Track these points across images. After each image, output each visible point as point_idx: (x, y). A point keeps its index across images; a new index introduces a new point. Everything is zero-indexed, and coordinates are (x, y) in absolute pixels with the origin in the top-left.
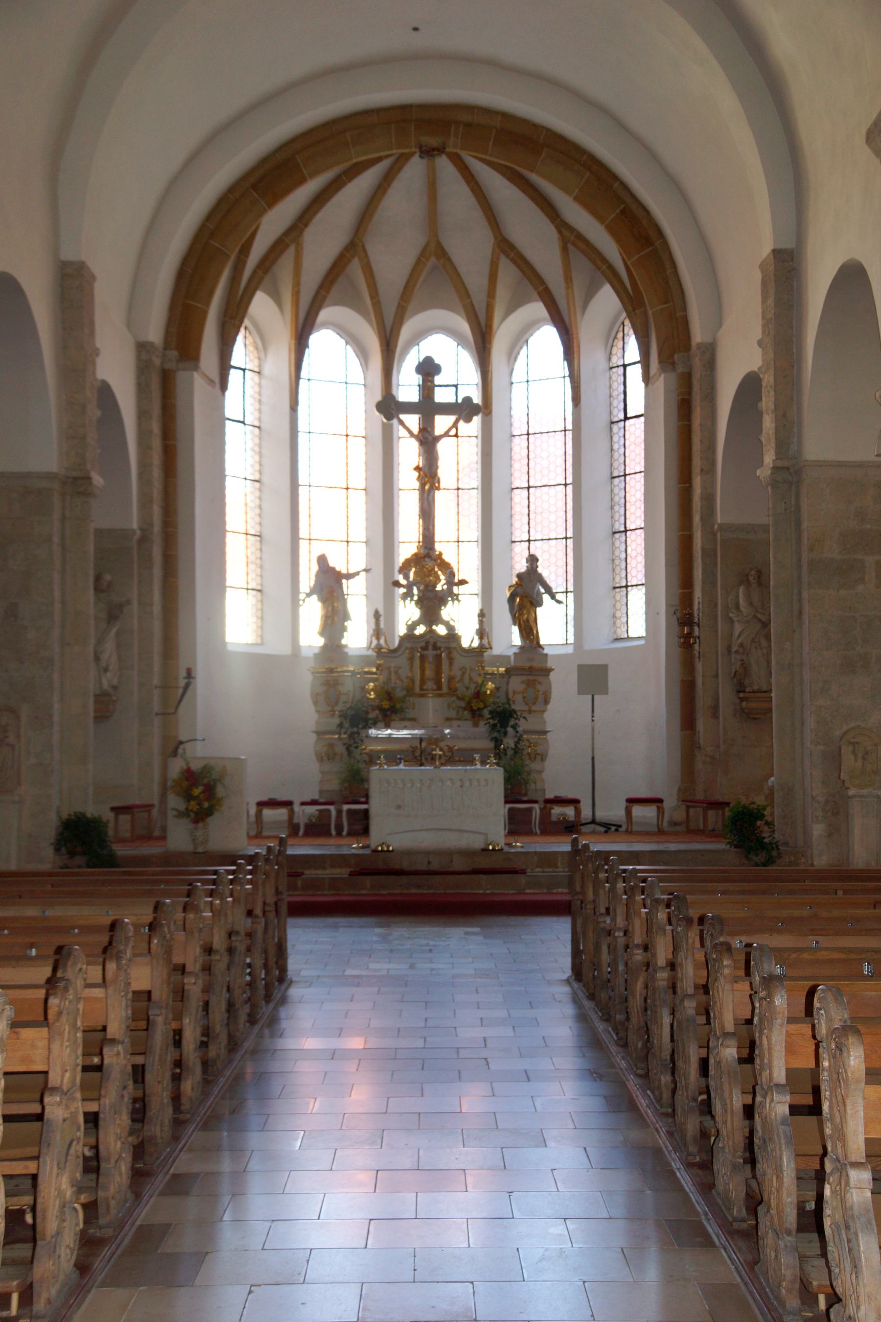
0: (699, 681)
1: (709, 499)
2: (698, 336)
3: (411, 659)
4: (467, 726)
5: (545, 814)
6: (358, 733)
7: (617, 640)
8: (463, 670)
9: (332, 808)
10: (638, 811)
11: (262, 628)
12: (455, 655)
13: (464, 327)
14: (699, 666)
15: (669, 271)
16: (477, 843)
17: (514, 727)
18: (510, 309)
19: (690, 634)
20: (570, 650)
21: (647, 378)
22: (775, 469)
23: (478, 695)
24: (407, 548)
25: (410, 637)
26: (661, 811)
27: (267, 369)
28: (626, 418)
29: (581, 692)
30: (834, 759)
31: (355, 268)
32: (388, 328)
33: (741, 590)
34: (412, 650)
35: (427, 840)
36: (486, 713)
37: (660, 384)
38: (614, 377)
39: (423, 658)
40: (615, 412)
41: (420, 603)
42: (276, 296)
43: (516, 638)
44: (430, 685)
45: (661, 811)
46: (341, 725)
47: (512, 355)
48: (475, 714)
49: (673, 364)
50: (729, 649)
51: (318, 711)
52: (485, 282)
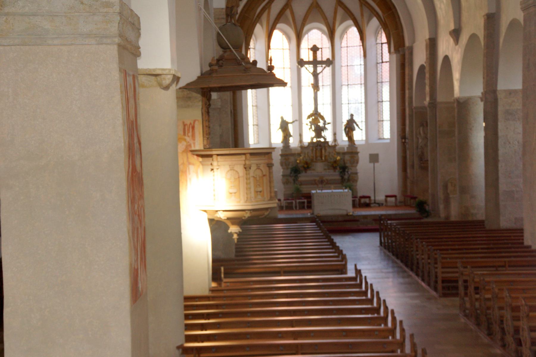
0: (408, 157)
1: (411, 98)
2: (407, 44)
3: (312, 150)
4: (331, 172)
5: (360, 200)
6: (297, 176)
7: (380, 139)
8: (330, 153)
9: (294, 202)
10: (389, 199)
11: (258, 138)
12: (327, 148)
13: (325, 28)
14: (408, 152)
15: (397, 20)
16: (344, 213)
17: (347, 172)
18: (341, 22)
19: (405, 142)
20: (364, 143)
21: (390, 52)
22: (429, 103)
23: (335, 162)
24: (308, 109)
25: (311, 144)
26: (396, 199)
27: (257, 48)
28: (382, 62)
29: (370, 162)
30: (446, 187)
31: (288, 12)
32: (298, 31)
33: (421, 128)
34: (313, 147)
35: (330, 212)
36: (338, 168)
37: (394, 56)
38: (378, 47)
39: (316, 149)
40: (378, 59)
41: (315, 131)
42: (262, 25)
43: (345, 138)
44: (319, 158)
45: (396, 199)
46: (291, 173)
47: (341, 37)
48: (335, 168)
49: (399, 51)
50: (417, 147)
51: (283, 169)
52: (332, 14)
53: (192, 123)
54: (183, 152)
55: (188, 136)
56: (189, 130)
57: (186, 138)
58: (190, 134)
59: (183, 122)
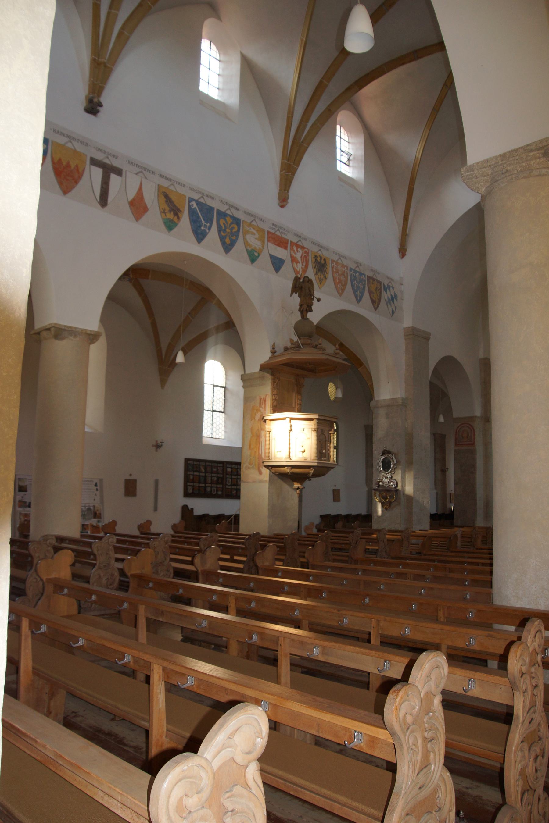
53: (265, 397)
54: (259, 420)
55: (262, 408)
56: (262, 403)
57: (261, 409)
58: (263, 406)
59: (260, 397)
